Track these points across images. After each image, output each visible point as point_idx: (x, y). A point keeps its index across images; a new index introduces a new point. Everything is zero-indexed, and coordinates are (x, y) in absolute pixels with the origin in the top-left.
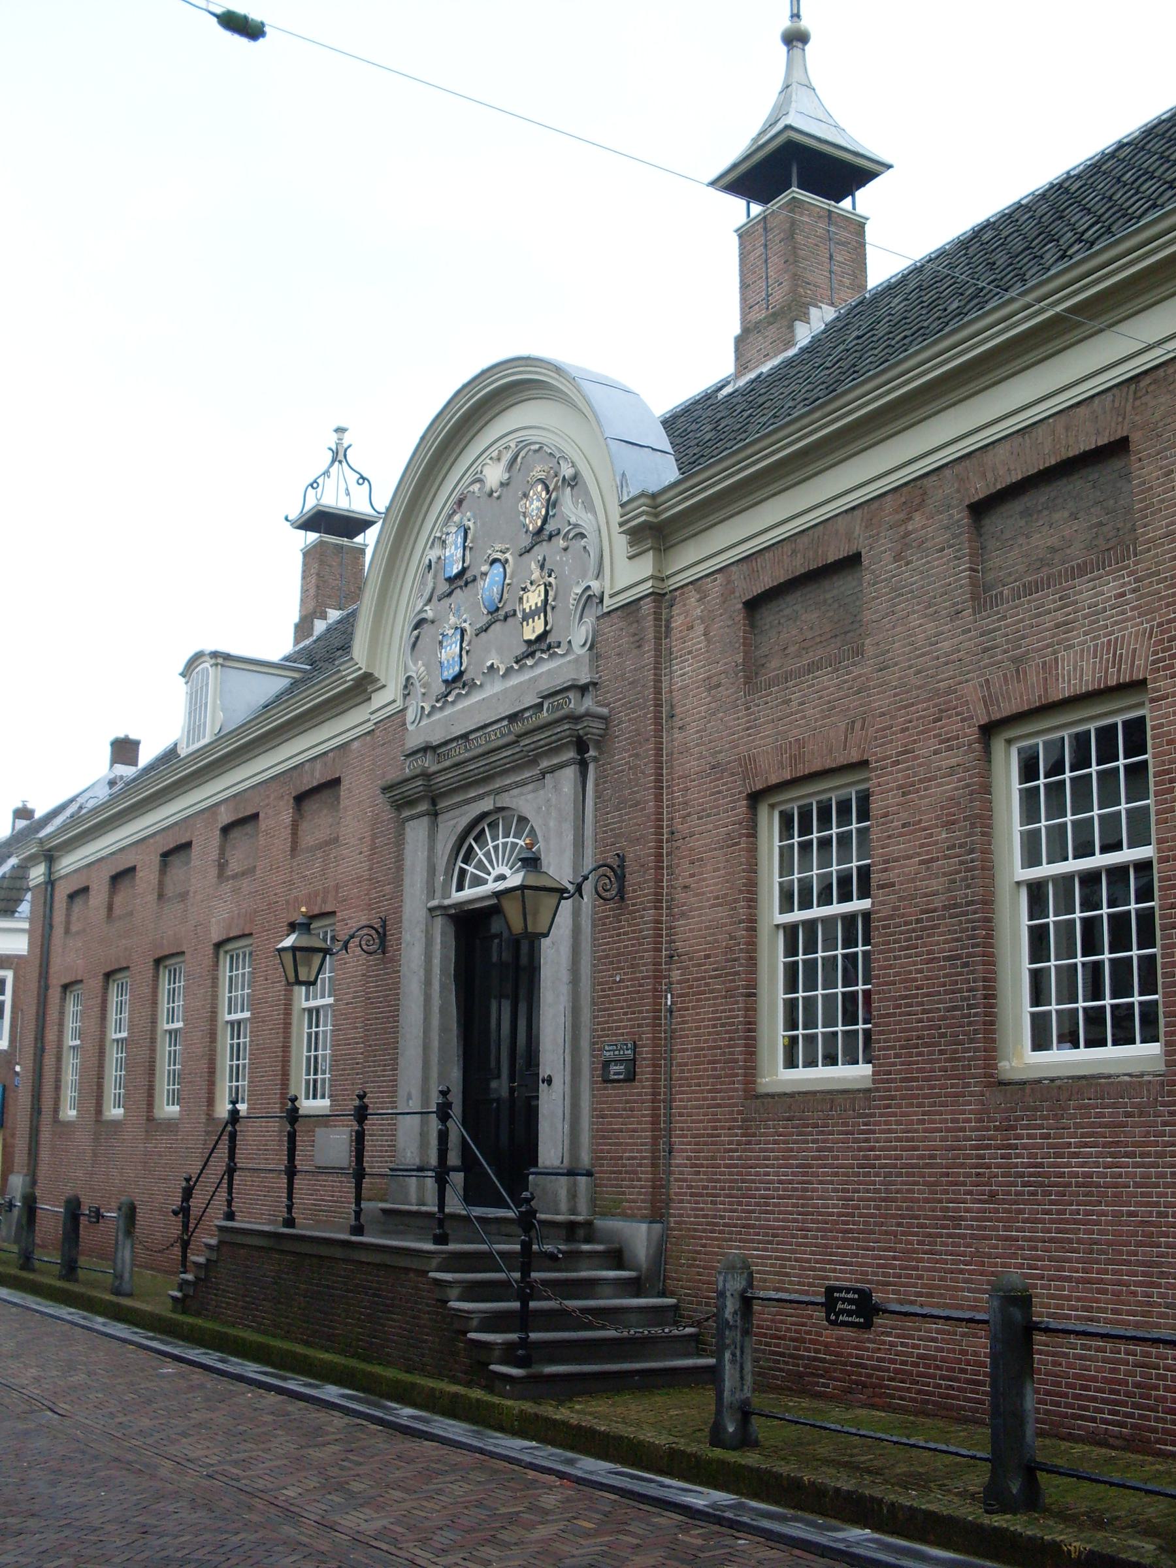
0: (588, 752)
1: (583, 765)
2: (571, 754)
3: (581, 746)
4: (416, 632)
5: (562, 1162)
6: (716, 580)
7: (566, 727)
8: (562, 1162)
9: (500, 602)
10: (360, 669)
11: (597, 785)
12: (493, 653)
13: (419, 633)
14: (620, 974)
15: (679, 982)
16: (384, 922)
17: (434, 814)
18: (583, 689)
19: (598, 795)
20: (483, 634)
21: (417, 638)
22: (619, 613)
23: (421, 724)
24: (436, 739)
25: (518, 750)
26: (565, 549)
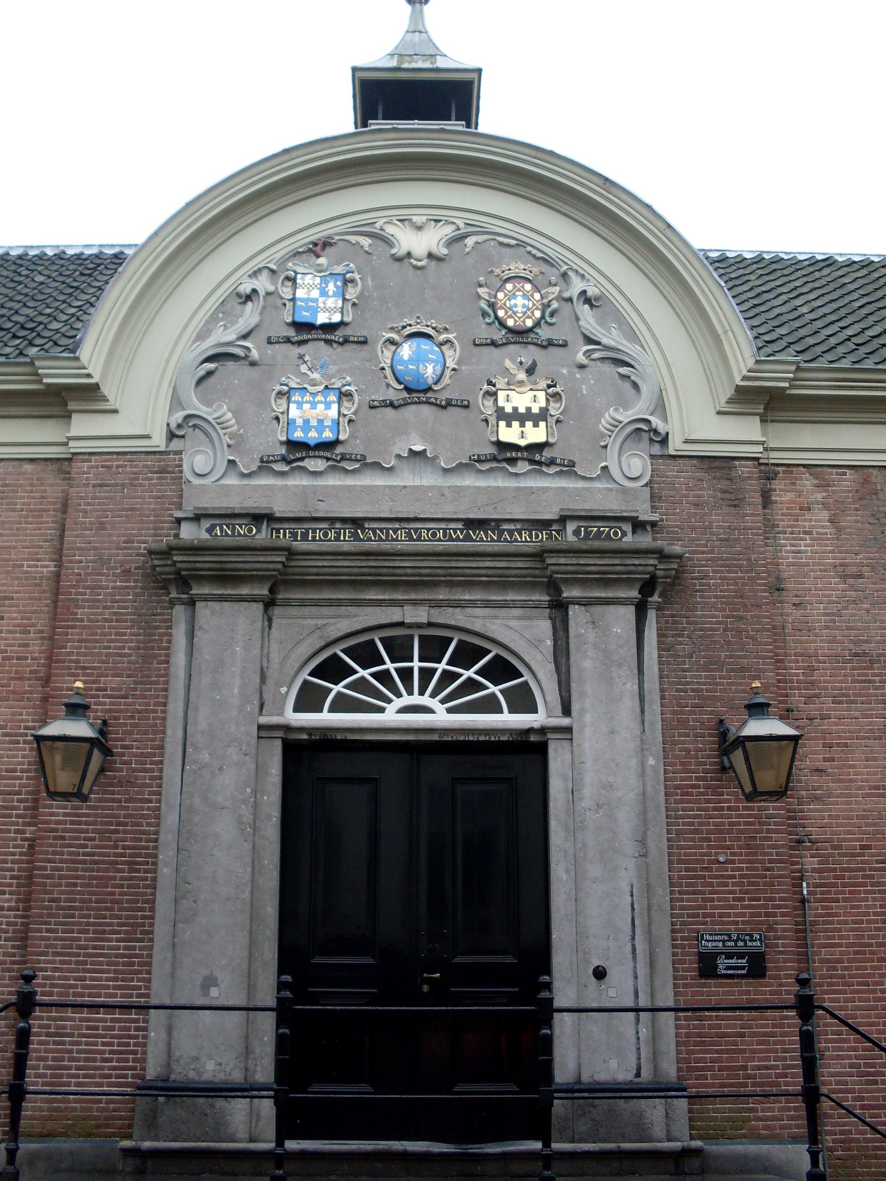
0: (651, 596)
1: (641, 609)
2: (634, 593)
3: (648, 587)
4: (210, 366)
5: (638, 1075)
6: (845, 474)
7: (651, 562)
8: (638, 1075)
9: (436, 384)
10: (89, 376)
11: (661, 635)
12: (414, 436)
13: (217, 368)
14: (726, 854)
15: (814, 870)
16: (105, 722)
17: (269, 604)
18: (638, 525)
19: (662, 647)
20: (389, 411)
21: (210, 374)
22: (695, 462)
23: (222, 482)
24: (280, 508)
25: (538, 565)
26: (582, 367)
